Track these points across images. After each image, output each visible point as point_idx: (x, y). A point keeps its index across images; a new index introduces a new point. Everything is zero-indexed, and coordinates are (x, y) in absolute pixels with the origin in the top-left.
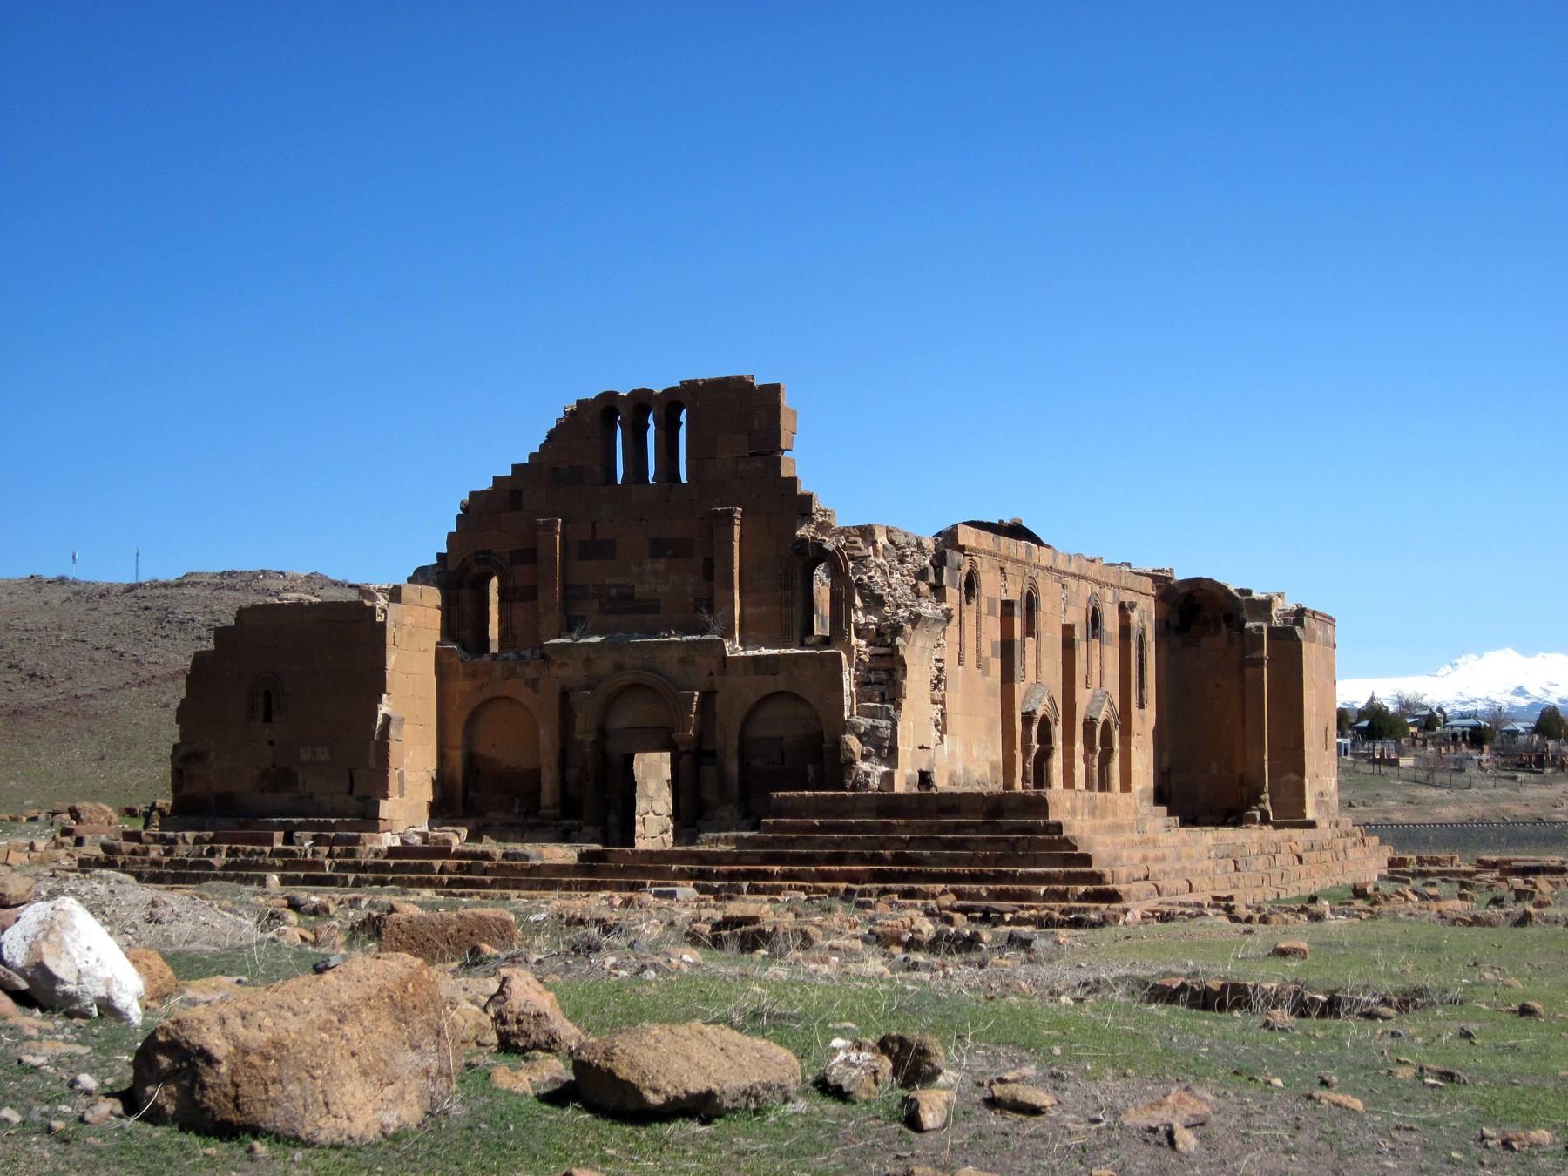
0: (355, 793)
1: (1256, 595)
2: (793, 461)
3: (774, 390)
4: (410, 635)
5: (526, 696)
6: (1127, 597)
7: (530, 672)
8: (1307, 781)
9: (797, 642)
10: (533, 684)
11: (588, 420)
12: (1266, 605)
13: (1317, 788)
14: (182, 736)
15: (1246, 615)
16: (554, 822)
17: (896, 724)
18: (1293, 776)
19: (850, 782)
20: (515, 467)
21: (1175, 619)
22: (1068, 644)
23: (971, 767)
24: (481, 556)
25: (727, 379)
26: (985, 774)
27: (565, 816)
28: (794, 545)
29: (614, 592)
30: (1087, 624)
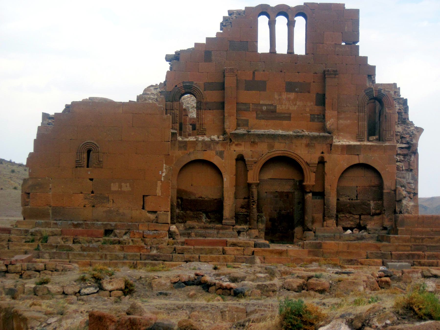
0: (147, 208)
3: (356, 12)
5: (216, 160)
7: (219, 148)
9: (366, 140)
10: (221, 154)
11: (251, 18)
14: (30, 174)
16: (232, 227)
19: (399, 209)
20: (208, 39)
24: (187, 84)
25: (331, 4)
27: (237, 223)
28: (365, 90)
29: (264, 108)
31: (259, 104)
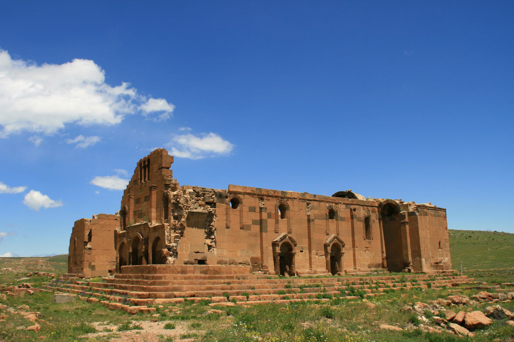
1: (404, 203)
2: (171, 171)
4: (102, 227)
6: (353, 207)
8: (423, 260)
12: (407, 206)
13: (433, 261)
15: (401, 210)
17: (177, 245)
18: (418, 258)
21: (386, 212)
22: (309, 221)
23: (235, 259)
25: (156, 150)
26: (247, 261)
29: (140, 212)
30: (326, 215)
31: (138, 211)
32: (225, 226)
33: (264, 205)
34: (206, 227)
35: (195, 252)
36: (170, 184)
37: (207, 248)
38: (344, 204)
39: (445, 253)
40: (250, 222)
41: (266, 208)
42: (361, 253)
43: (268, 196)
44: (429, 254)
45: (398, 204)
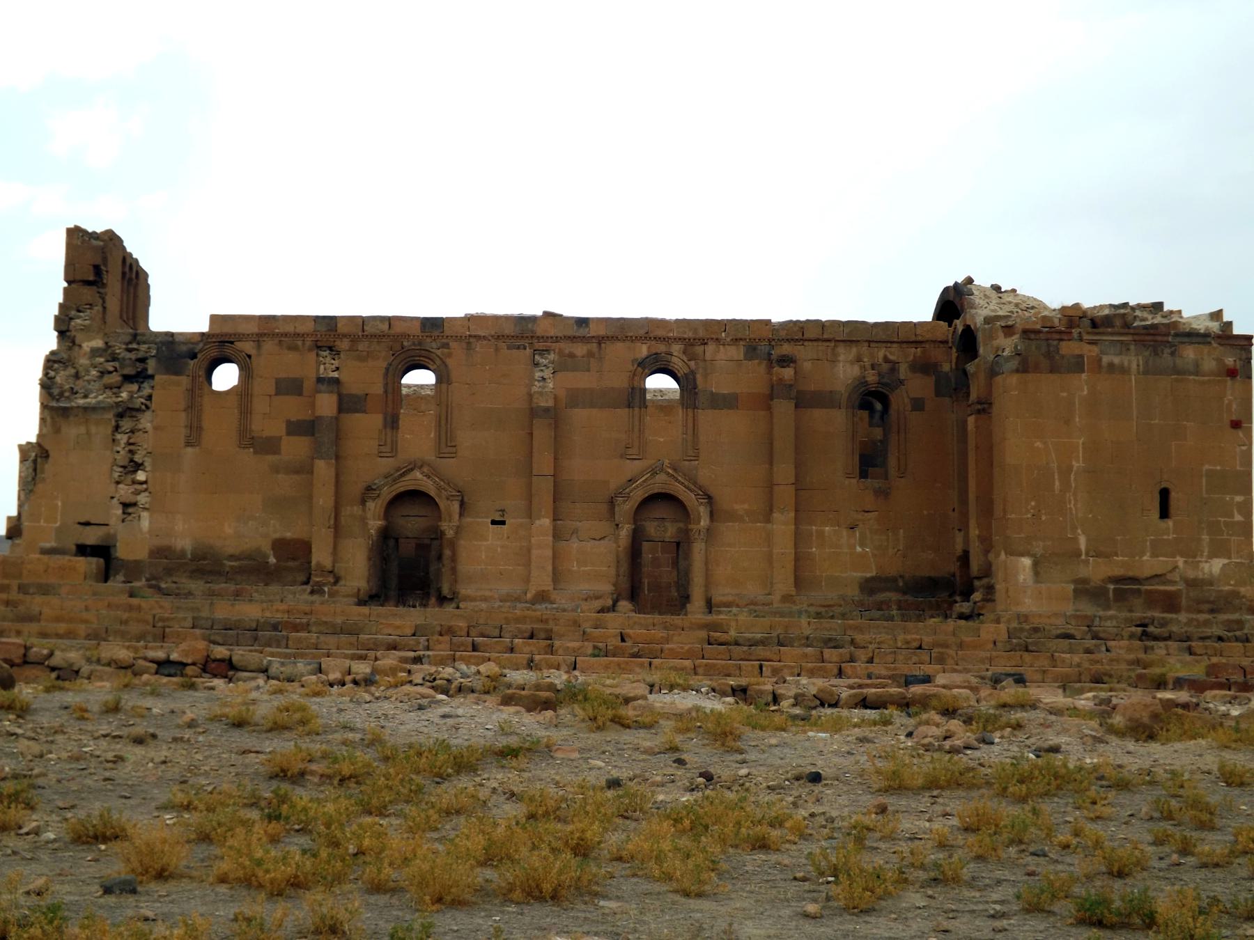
15: (981, 351)
18: (1003, 556)
32: (183, 444)
33: (337, 369)
34: (119, 449)
35: (80, 523)
36: (68, 331)
37: (120, 512)
38: (736, 340)
39: (1206, 537)
40: (276, 428)
41: (337, 381)
42: (821, 534)
43: (354, 339)
44: (1075, 540)
45: (977, 330)
